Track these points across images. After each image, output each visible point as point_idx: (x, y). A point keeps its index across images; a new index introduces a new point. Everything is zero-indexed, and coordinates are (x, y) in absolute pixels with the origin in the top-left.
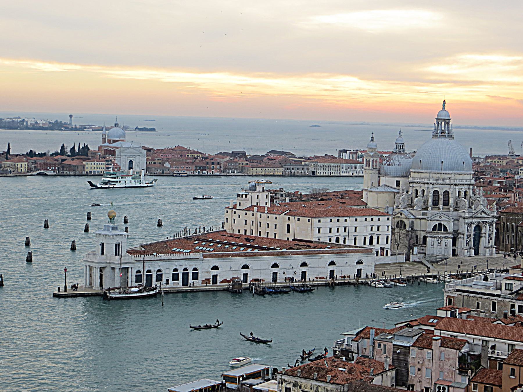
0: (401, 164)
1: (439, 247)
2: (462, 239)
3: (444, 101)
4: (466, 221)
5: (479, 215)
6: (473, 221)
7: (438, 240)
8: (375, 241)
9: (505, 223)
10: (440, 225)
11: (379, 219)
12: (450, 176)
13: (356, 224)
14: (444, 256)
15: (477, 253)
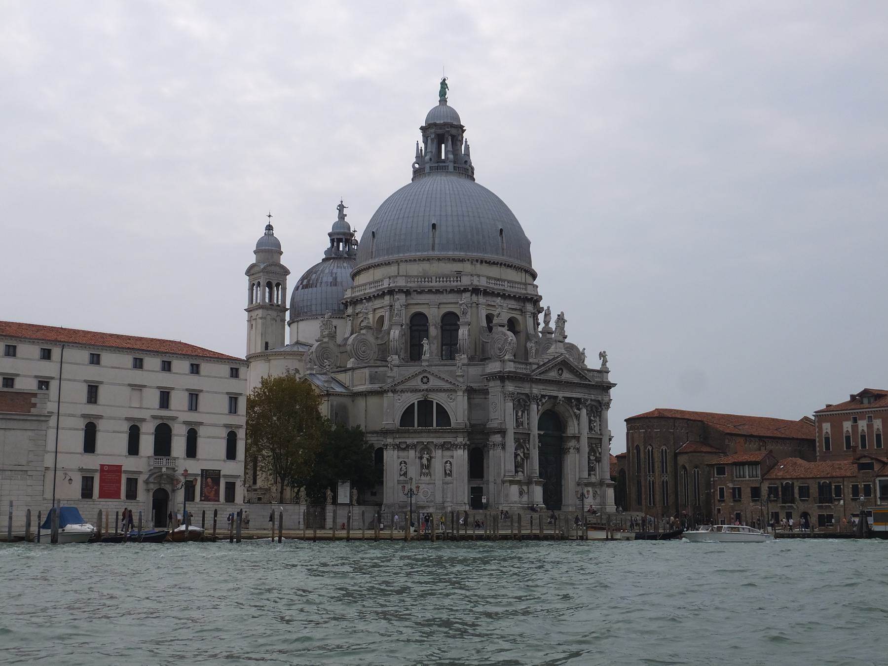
0: (339, 280)
1: (423, 478)
2: (499, 451)
3: (444, 84)
4: (510, 387)
5: (553, 375)
6: (535, 391)
7: (421, 458)
8: (179, 446)
9: (642, 448)
10: (425, 405)
11: (195, 369)
12: (458, 267)
13: (93, 373)
14: (444, 508)
15: (554, 498)
